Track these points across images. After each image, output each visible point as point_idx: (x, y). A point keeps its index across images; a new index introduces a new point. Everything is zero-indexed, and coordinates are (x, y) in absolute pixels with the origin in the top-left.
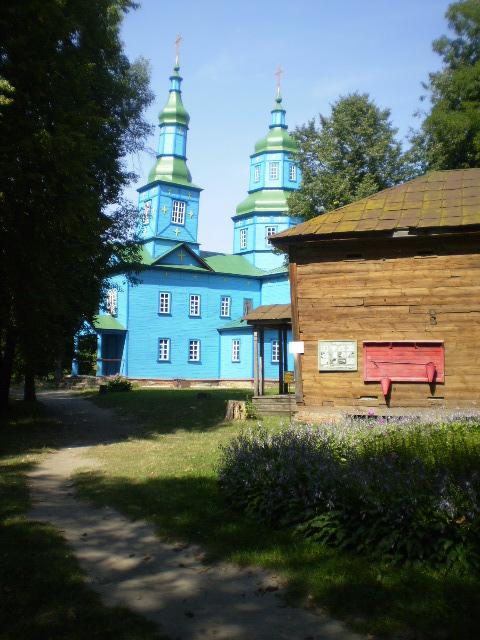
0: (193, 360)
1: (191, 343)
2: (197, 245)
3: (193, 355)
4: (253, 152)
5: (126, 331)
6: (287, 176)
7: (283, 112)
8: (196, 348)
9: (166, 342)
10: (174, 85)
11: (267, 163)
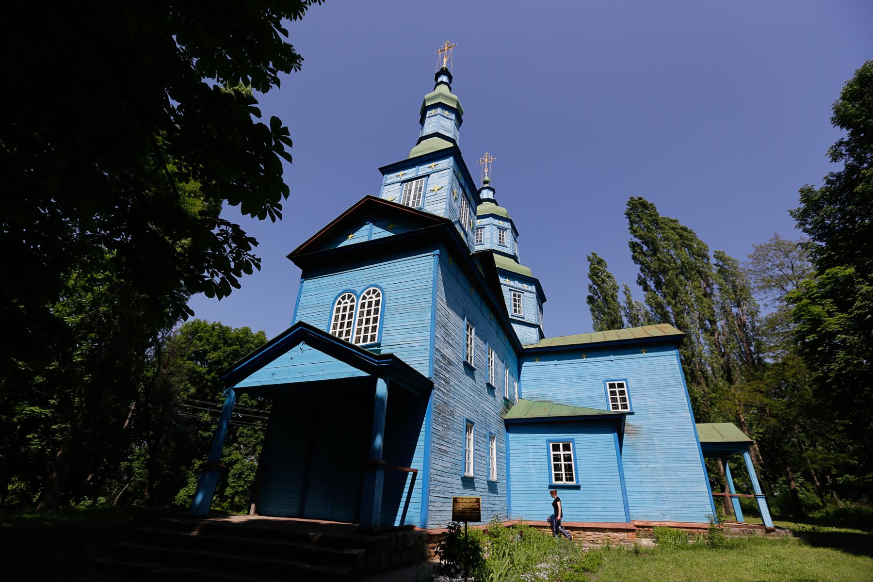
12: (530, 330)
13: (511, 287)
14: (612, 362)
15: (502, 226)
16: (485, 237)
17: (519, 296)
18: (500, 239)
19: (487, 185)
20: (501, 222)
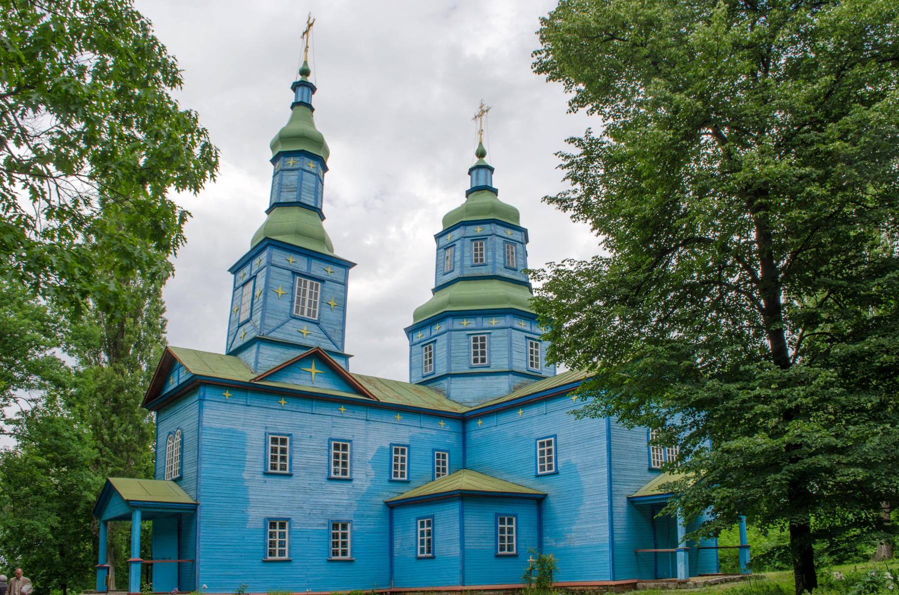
0: (340, 557)
1: (335, 526)
2: (347, 357)
3: (340, 549)
4: (440, 228)
8: (344, 536)
17: (483, 339)
18: (476, 255)
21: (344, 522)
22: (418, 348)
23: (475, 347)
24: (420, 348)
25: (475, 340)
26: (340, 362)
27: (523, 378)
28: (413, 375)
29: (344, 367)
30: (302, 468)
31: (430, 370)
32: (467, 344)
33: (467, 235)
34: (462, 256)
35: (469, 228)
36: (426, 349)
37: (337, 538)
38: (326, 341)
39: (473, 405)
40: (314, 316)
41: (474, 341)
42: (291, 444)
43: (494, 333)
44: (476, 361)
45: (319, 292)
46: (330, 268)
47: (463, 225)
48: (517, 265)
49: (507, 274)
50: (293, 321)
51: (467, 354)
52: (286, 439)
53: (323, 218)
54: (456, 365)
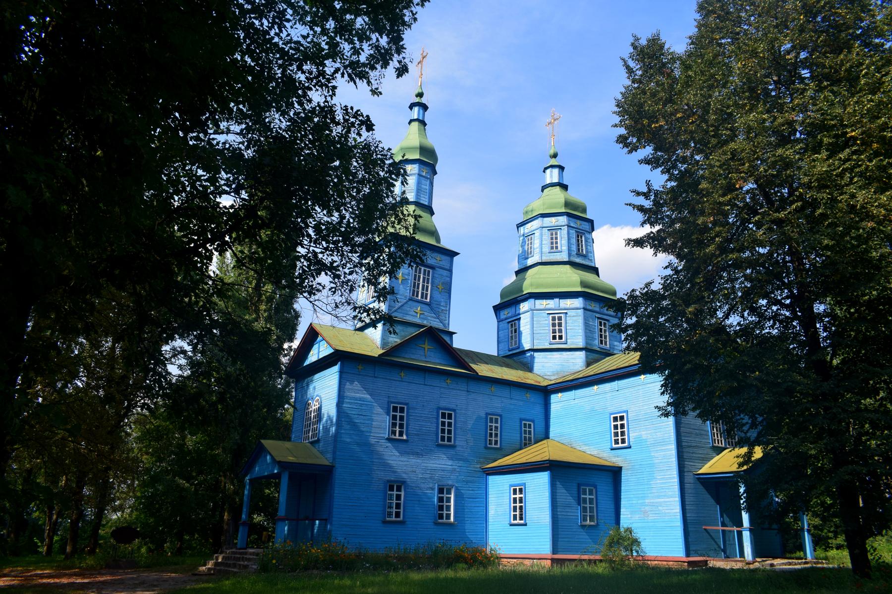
1: (441, 491)
2: (451, 334)
5: (333, 467)
6: (574, 248)
7: (561, 168)
9: (399, 489)
10: (416, 113)
11: (545, 230)
12: (573, 356)
13: (550, 310)
14: (618, 393)
15: (556, 224)
16: (535, 246)
17: (560, 318)
18: (552, 243)
19: (554, 162)
20: (553, 219)
21: (448, 487)
22: (504, 324)
23: (554, 325)
24: (506, 325)
25: (554, 319)
26: (447, 338)
27: (594, 355)
28: (500, 348)
29: (449, 342)
30: (417, 435)
31: (515, 344)
32: (547, 322)
33: (544, 225)
34: (541, 244)
35: (545, 219)
36: (512, 325)
37: (443, 502)
38: (435, 319)
39: (553, 378)
40: (426, 298)
41: (553, 320)
42: (408, 412)
43: (570, 313)
44: (554, 337)
45: (430, 277)
46: (439, 257)
47: (541, 217)
48: (587, 252)
49: (578, 260)
50: (410, 303)
51: (547, 331)
52: (404, 408)
53: (432, 213)
54: (538, 341)
